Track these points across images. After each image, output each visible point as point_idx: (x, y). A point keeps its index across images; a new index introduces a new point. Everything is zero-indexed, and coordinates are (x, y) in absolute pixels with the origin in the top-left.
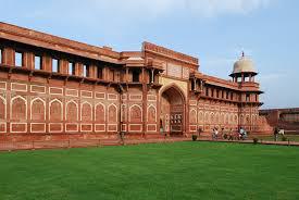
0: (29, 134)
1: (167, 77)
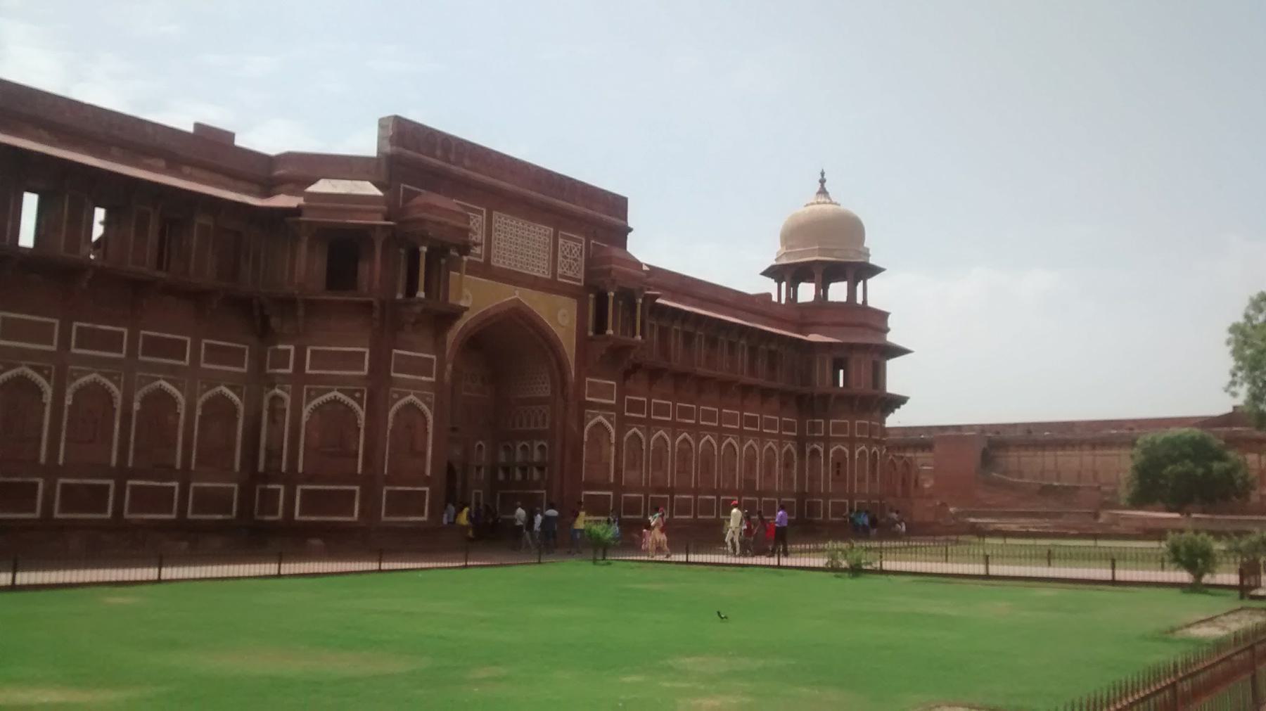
1: (485, 270)
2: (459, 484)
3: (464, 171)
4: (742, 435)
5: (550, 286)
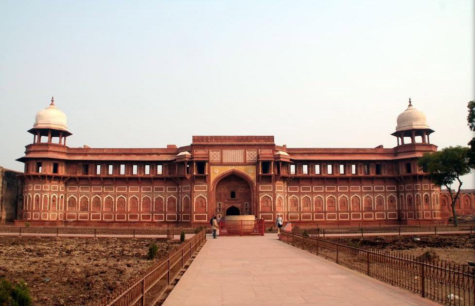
0: (102, 222)
1: (221, 164)
2: (241, 213)
3: (211, 143)
4: (361, 193)
5: (245, 164)
